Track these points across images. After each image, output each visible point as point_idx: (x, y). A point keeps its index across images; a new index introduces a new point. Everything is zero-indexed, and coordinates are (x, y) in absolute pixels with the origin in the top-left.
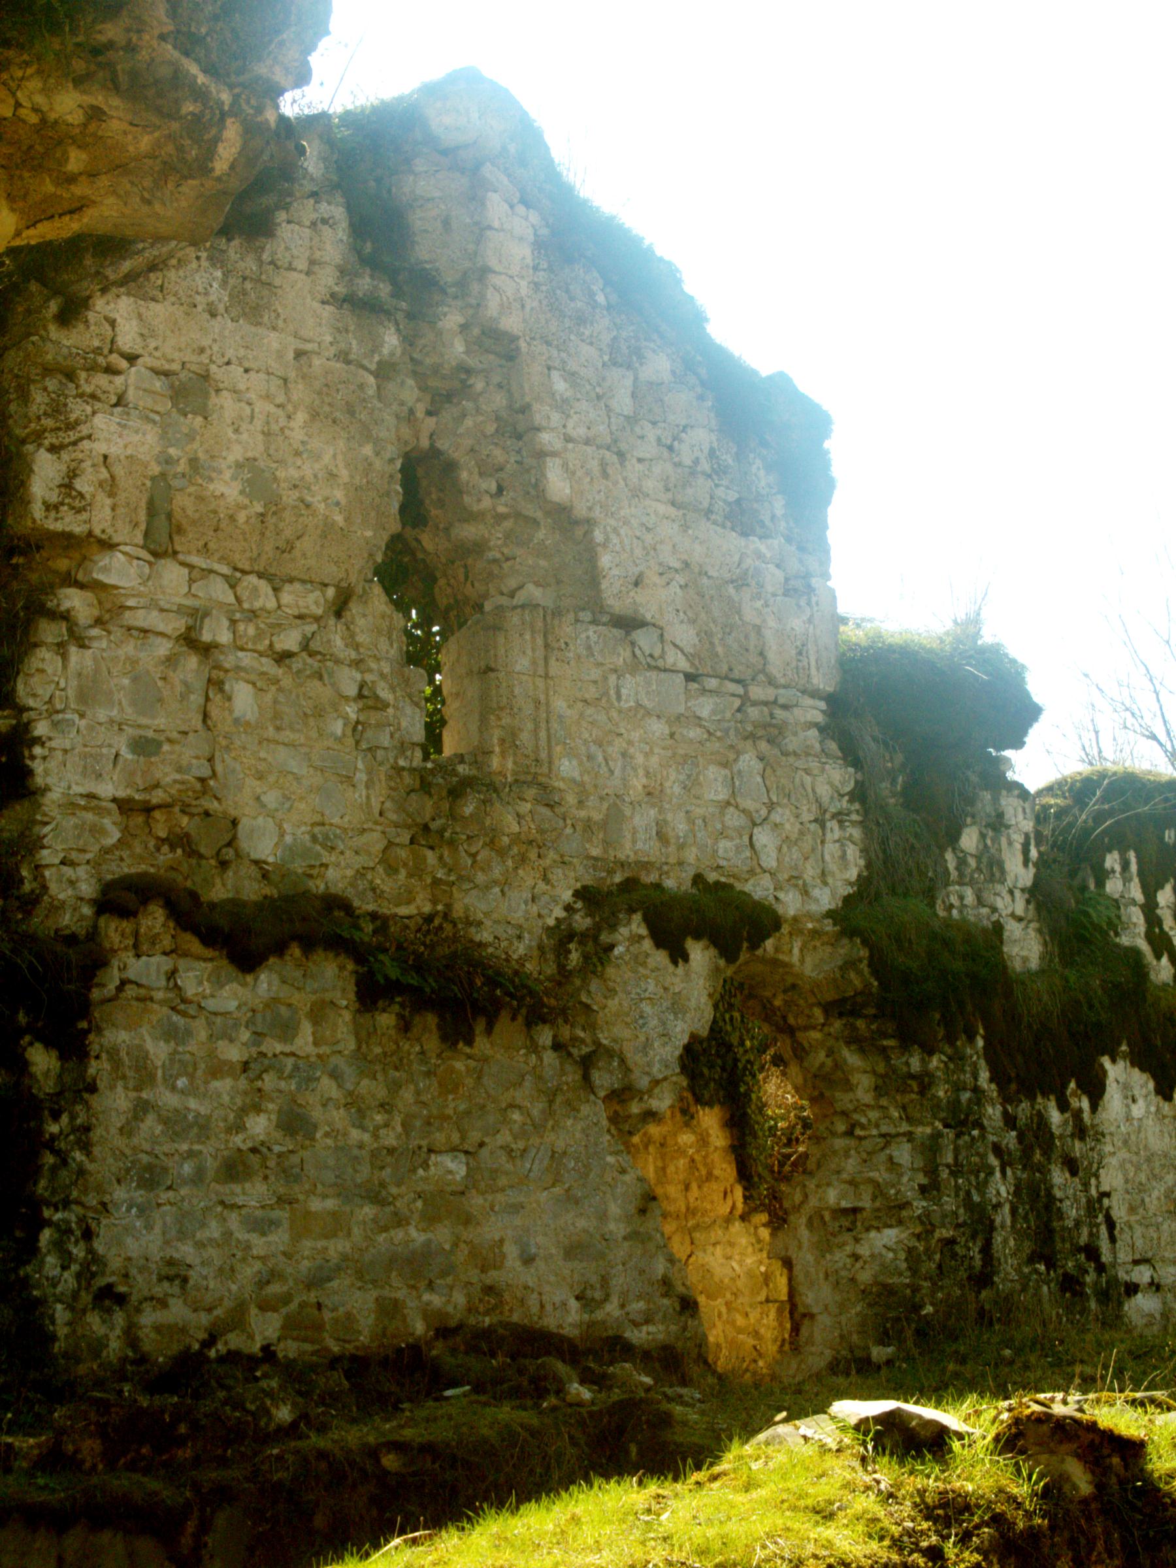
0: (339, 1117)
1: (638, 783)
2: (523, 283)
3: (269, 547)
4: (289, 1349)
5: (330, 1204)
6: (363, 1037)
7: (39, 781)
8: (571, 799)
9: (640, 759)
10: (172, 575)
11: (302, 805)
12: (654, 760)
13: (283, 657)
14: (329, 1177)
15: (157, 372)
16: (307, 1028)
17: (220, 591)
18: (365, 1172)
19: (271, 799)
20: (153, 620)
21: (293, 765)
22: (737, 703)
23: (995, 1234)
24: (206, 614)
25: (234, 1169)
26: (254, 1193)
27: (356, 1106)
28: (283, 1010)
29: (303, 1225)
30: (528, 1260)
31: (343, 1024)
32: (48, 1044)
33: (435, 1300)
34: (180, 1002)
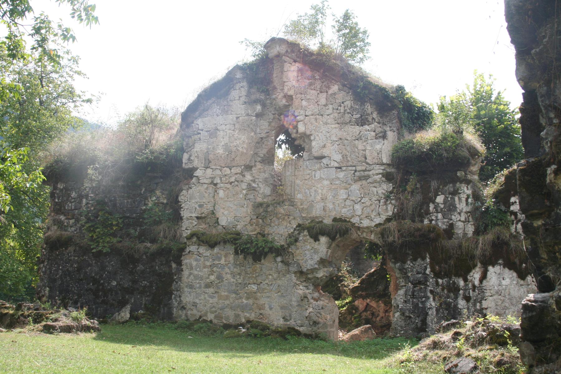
0: (229, 276)
1: (319, 198)
2: (294, 82)
3: (229, 161)
4: (215, 321)
5: (226, 293)
7: (182, 215)
8: (299, 204)
9: (320, 191)
10: (209, 171)
11: (233, 213)
12: (325, 191)
13: (231, 183)
14: (226, 288)
15: (207, 131)
16: (223, 259)
17: (218, 172)
19: (226, 213)
21: (231, 205)
22: (353, 172)
23: (428, 317)
24: (215, 178)
25: (208, 286)
26: (211, 290)
27: (233, 275)
28: (219, 255)
29: (220, 297)
30: (271, 309)
31: (231, 258)
32: (175, 263)
33: (248, 315)
34: (199, 255)
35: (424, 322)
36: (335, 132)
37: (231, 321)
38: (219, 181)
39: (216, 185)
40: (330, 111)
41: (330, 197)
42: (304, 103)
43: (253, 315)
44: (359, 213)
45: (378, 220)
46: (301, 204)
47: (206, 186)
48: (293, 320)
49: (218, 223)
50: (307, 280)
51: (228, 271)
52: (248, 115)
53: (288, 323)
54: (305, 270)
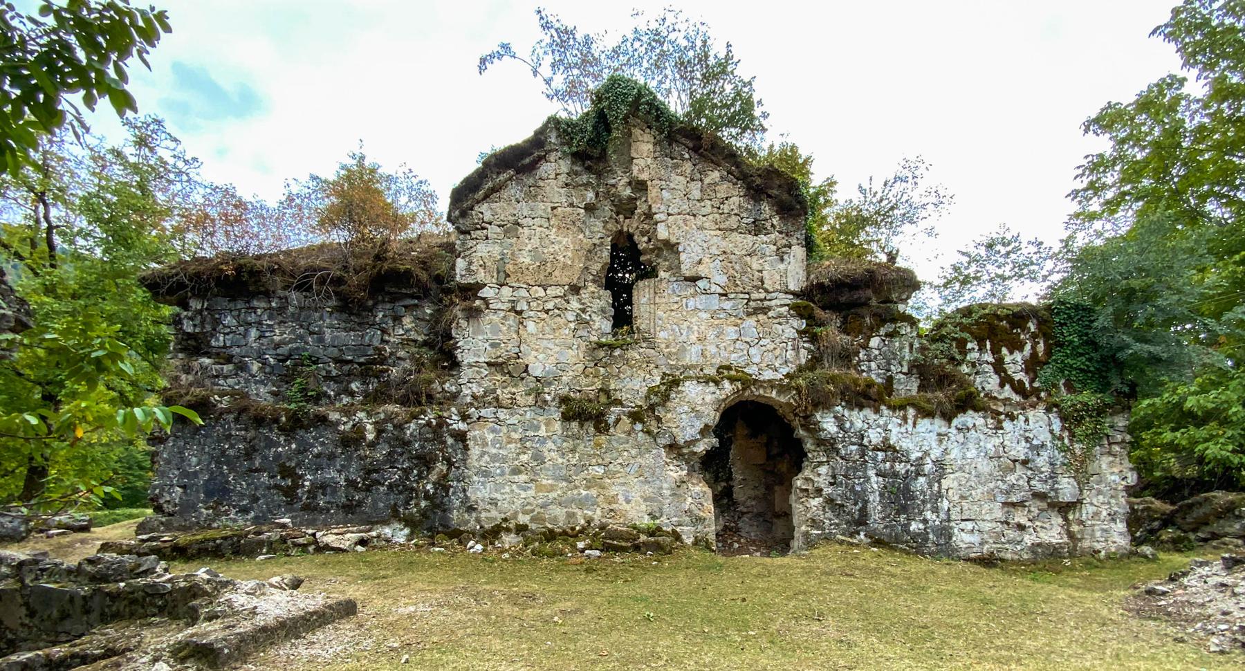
1: (693, 338)
4: (533, 526)
6: (564, 429)
9: (696, 328)
10: (506, 291)
12: (703, 328)
13: (547, 312)
16: (543, 428)
17: (523, 293)
18: (564, 472)
20: (500, 306)
25: (516, 471)
26: (523, 478)
31: (557, 426)
33: (590, 513)
34: (498, 421)
35: (863, 511)
36: (717, 242)
37: (561, 524)
38: (525, 307)
39: (519, 313)
40: (709, 209)
41: (711, 335)
42: (665, 194)
43: (599, 512)
44: (756, 360)
45: (785, 371)
46: (667, 347)
47: (502, 314)
48: (664, 519)
49: (526, 371)
50: (680, 456)
51: (554, 447)
52: (572, 205)
53: (658, 521)
54: (682, 442)
